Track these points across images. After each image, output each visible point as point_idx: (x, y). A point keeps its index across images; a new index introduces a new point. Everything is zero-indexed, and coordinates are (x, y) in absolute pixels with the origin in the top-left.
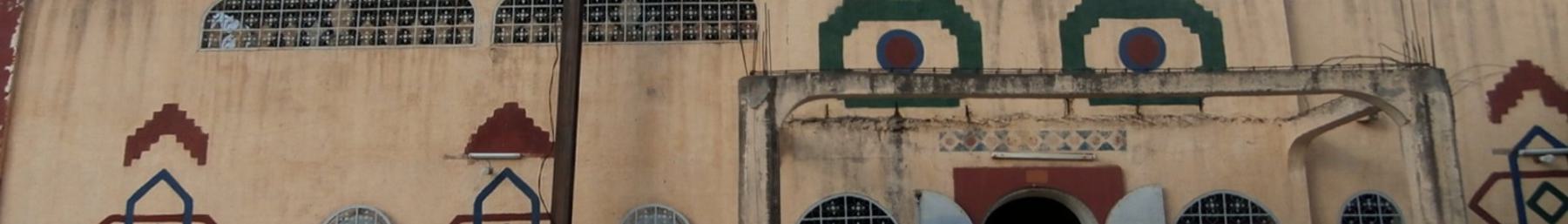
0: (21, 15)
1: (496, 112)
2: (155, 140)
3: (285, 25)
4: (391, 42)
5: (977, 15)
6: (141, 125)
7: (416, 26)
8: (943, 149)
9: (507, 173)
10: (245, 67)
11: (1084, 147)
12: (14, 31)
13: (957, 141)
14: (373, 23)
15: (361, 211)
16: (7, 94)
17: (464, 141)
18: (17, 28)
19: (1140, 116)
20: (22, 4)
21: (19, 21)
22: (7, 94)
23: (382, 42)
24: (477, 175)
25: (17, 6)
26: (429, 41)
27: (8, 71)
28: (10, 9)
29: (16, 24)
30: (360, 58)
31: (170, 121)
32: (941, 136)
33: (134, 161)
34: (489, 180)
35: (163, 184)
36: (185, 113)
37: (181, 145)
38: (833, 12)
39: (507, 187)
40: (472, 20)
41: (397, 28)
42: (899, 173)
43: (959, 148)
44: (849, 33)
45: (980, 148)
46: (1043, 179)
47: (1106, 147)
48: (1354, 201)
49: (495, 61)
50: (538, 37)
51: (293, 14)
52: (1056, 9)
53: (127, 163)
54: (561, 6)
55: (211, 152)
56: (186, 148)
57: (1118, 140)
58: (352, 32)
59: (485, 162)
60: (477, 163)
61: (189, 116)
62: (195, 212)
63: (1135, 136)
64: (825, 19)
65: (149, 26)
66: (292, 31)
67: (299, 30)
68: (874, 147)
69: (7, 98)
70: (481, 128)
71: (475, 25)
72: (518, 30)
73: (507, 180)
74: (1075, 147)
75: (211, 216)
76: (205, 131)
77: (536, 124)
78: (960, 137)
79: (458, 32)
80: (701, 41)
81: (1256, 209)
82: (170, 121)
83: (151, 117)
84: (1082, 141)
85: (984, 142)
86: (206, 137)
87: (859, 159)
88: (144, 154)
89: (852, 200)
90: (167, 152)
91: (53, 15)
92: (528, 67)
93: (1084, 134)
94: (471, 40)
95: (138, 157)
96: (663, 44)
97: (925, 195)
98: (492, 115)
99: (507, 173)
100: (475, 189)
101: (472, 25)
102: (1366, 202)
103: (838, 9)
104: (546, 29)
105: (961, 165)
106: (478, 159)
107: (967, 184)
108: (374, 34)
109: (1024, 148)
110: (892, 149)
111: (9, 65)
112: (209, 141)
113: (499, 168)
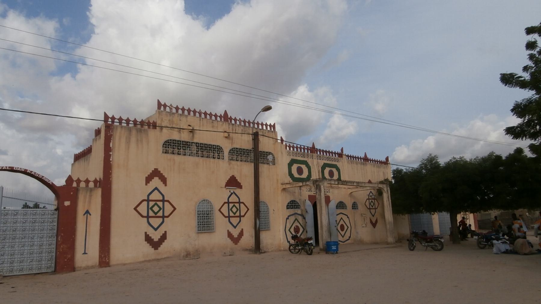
2: (153, 178)
5: (310, 165)
6: (149, 174)
8: (307, 191)
9: (234, 193)
10: (174, 160)
12: (111, 142)
13: (309, 190)
14: (207, 152)
15: (204, 200)
17: (224, 184)
18: (112, 141)
19: (331, 186)
20: (112, 133)
21: (112, 138)
22: (111, 161)
25: (111, 134)
27: (110, 154)
28: (109, 134)
31: (156, 173)
32: (306, 188)
33: (148, 184)
34: (230, 193)
37: (160, 180)
38: (290, 161)
42: (301, 195)
43: (309, 191)
44: (292, 166)
45: (312, 191)
47: (327, 192)
49: (229, 165)
50: (201, 156)
52: (321, 165)
53: (146, 184)
55: (168, 182)
57: (329, 191)
59: (229, 189)
60: (227, 189)
63: (331, 190)
68: (297, 190)
69: (111, 162)
70: (228, 181)
75: (169, 200)
77: (238, 181)
78: (309, 189)
79: (209, 155)
80: (182, 155)
82: (156, 173)
83: (151, 172)
85: (312, 190)
88: (150, 182)
89: (294, 201)
90: (156, 182)
95: (149, 183)
97: (306, 200)
98: (229, 178)
100: (228, 195)
103: (291, 161)
105: (309, 194)
106: (227, 188)
108: (166, 150)
110: (299, 190)
111: (111, 152)
113: (232, 191)
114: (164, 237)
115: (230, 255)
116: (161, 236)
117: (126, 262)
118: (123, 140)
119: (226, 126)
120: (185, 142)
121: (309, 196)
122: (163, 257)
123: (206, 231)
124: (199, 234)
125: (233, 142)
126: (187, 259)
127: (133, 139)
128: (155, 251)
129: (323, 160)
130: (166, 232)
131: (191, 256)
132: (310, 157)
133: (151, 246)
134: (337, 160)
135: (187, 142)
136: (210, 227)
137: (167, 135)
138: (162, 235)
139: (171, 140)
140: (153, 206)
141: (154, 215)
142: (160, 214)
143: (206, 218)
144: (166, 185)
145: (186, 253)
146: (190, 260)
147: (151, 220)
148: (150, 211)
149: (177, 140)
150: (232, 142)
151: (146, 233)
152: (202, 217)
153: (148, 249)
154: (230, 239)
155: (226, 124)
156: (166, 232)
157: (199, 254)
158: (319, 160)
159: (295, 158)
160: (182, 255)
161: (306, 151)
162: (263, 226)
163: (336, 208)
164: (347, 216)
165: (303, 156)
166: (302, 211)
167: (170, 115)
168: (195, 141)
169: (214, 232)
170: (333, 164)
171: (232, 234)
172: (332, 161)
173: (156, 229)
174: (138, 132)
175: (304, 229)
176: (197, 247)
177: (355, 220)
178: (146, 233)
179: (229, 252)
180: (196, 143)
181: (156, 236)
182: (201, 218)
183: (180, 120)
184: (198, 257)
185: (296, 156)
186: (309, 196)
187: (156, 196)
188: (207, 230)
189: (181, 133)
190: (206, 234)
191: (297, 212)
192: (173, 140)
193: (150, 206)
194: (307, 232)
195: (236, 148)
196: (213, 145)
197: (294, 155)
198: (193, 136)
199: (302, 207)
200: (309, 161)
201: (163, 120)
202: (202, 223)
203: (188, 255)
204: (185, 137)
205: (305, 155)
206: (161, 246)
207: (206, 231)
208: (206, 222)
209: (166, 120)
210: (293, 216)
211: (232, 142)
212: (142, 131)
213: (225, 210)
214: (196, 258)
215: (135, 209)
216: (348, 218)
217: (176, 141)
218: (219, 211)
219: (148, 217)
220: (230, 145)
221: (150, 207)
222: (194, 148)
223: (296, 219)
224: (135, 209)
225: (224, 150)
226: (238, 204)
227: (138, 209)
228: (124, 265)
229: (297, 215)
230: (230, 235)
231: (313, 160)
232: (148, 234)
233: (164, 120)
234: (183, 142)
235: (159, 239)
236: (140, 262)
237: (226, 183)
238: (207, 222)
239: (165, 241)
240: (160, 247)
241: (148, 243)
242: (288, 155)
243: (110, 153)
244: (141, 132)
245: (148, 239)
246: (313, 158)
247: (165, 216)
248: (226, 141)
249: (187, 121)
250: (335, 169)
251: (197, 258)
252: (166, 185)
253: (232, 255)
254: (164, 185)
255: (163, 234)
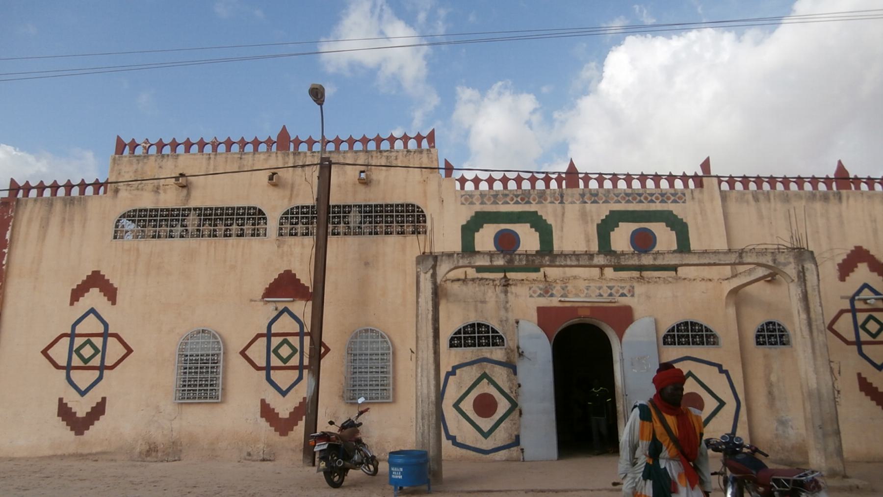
0: (12, 221)
1: (279, 275)
2: (88, 291)
3: (161, 226)
4: (220, 236)
5: (550, 220)
6: (80, 283)
7: (234, 227)
8: (531, 296)
9: (286, 310)
10: (138, 250)
11: (611, 295)
12: (8, 230)
13: (539, 292)
14: (210, 225)
15: (203, 331)
16: (4, 265)
17: (261, 291)
18: (10, 228)
19: (642, 277)
20: (13, 214)
21: (11, 224)
22: (4, 265)
23: (215, 236)
24: (268, 311)
26: (242, 235)
27: (4, 252)
28: (6, 217)
29: (9, 226)
30: (203, 244)
31: (96, 280)
32: (530, 289)
33: (75, 303)
34: (275, 313)
35: (92, 315)
36: (104, 276)
39: (285, 317)
40: (266, 223)
41: (223, 228)
42: (506, 309)
43: (540, 295)
44: (478, 231)
45: (552, 295)
46: (587, 313)
47: (623, 295)
48: (763, 325)
49: (278, 247)
50: (303, 233)
51: (165, 220)
53: (72, 304)
54: (316, 215)
56: (105, 295)
57: (629, 291)
58: (198, 230)
59: (273, 303)
60: (268, 304)
61: (106, 278)
62: (110, 332)
63: (639, 289)
64: (464, 223)
65: (84, 227)
66: (164, 230)
67: (169, 229)
68: (492, 295)
69: (4, 267)
70: (271, 284)
71: (268, 226)
72: (292, 229)
73: (286, 313)
74: (605, 295)
76: (115, 286)
77: (302, 282)
78: (541, 289)
79: (258, 230)
80: (394, 235)
81: (707, 330)
82: (96, 280)
83: (85, 278)
84: (609, 291)
85: (554, 292)
86: (116, 289)
87: (484, 302)
88: (81, 299)
89: (480, 325)
90: (94, 298)
91: (30, 221)
92: (297, 250)
93: (610, 288)
94: (265, 235)
95: (78, 300)
96: (374, 237)
97: (521, 322)
98: (277, 277)
99: (286, 310)
101: (265, 226)
102: (759, 339)
103: (472, 217)
104: (307, 229)
105: (541, 305)
107: (545, 316)
109: (577, 295)
110: (502, 296)
111: (5, 249)
112: (118, 292)
113: (281, 307)
114: (99, 410)
115: (264, 460)
116: (92, 408)
117: (16, 455)
118: (35, 226)
119: (277, 160)
120: (167, 210)
121: (541, 311)
122: (94, 451)
123: (208, 401)
124: (184, 406)
125: (295, 192)
126: (148, 459)
127: (55, 220)
128: (77, 436)
129: (606, 202)
130: (104, 399)
131: (160, 454)
132: (549, 200)
133: (69, 428)
134: (673, 198)
135: (173, 210)
136: (208, 392)
137: (127, 201)
138: (94, 405)
139: (135, 211)
140: (82, 346)
141: (82, 364)
142: (96, 362)
143: (199, 370)
144: (114, 303)
145: (148, 447)
146: (156, 461)
147: (75, 375)
148: (75, 356)
149: (150, 209)
150: (291, 195)
151: (61, 400)
152: (190, 368)
153: (63, 432)
154: (267, 420)
155: (277, 156)
156: (104, 399)
157: (181, 451)
158: (589, 206)
159: (489, 208)
160: (138, 450)
161: (554, 185)
162: (379, 392)
163: (665, 343)
164: (719, 367)
165: (522, 199)
166: (509, 351)
167: (137, 160)
168: (192, 204)
169: (221, 402)
170: (651, 209)
171: (274, 409)
172: (652, 201)
173: (83, 393)
174: (65, 205)
175: (514, 405)
176: (174, 434)
177: (773, 378)
178: (61, 400)
179: (261, 453)
180: (195, 209)
181: (81, 407)
182: (187, 371)
183: (160, 167)
184: (176, 458)
185: (495, 203)
186: (541, 311)
187: (91, 325)
188: (211, 398)
189: (159, 193)
190: (200, 406)
191: (488, 355)
192: (141, 210)
193: (75, 347)
194: (521, 414)
195: (303, 207)
196: (239, 208)
197: (485, 200)
198: (188, 195)
199: (509, 343)
200: (548, 212)
201: (123, 173)
202: (211, 381)
203: (151, 451)
204: (170, 199)
205: (532, 197)
206: (91, 427)
207: (208, 401)
208: (209, 379)
209: (128, 172)
210: (475, 367)
211: (291, 195)
212: (76, 202)
213: (258, 353)
214: (170, 459)
215: (45, 352)
216: (724, 375)
217: (146, 210)
218: (240, 356)
219: (69, 368)
220: (286, 201)
221: (74, 349)
222: (192, 221)
223: (484, 376)
224: (45, 352)
225: (267, 216)
226: (273, 338)
227: (50, 352)
228: (11, 459)
229: (489, 365)
230: (267, 412)
231: (564, 208)
232: (64, 401)
233: (125, 172)
234: (162, 210)
235: (87, 413)
236: (42, 458)
237: (267, 289)
238: (211, 381)
239: (101, 417)
240: (88, 429)
241: (63, 420)
242: (462, 204)
243: (4, 250)
244: (73, 204)
245: (65, 412)
246: (562, 202)
247: (106, 366)
248: (274, 193)
249: (176, 166)
250: (662, 225)
251: (174, 459)
252: (114, 303)
253: (270, 460)
254: (110, 302)
255: (98, 403)
